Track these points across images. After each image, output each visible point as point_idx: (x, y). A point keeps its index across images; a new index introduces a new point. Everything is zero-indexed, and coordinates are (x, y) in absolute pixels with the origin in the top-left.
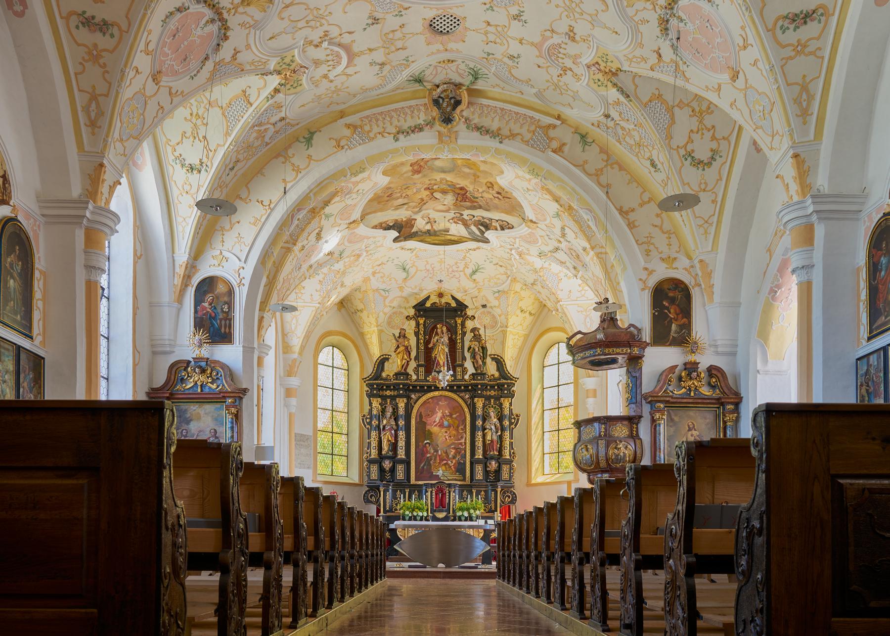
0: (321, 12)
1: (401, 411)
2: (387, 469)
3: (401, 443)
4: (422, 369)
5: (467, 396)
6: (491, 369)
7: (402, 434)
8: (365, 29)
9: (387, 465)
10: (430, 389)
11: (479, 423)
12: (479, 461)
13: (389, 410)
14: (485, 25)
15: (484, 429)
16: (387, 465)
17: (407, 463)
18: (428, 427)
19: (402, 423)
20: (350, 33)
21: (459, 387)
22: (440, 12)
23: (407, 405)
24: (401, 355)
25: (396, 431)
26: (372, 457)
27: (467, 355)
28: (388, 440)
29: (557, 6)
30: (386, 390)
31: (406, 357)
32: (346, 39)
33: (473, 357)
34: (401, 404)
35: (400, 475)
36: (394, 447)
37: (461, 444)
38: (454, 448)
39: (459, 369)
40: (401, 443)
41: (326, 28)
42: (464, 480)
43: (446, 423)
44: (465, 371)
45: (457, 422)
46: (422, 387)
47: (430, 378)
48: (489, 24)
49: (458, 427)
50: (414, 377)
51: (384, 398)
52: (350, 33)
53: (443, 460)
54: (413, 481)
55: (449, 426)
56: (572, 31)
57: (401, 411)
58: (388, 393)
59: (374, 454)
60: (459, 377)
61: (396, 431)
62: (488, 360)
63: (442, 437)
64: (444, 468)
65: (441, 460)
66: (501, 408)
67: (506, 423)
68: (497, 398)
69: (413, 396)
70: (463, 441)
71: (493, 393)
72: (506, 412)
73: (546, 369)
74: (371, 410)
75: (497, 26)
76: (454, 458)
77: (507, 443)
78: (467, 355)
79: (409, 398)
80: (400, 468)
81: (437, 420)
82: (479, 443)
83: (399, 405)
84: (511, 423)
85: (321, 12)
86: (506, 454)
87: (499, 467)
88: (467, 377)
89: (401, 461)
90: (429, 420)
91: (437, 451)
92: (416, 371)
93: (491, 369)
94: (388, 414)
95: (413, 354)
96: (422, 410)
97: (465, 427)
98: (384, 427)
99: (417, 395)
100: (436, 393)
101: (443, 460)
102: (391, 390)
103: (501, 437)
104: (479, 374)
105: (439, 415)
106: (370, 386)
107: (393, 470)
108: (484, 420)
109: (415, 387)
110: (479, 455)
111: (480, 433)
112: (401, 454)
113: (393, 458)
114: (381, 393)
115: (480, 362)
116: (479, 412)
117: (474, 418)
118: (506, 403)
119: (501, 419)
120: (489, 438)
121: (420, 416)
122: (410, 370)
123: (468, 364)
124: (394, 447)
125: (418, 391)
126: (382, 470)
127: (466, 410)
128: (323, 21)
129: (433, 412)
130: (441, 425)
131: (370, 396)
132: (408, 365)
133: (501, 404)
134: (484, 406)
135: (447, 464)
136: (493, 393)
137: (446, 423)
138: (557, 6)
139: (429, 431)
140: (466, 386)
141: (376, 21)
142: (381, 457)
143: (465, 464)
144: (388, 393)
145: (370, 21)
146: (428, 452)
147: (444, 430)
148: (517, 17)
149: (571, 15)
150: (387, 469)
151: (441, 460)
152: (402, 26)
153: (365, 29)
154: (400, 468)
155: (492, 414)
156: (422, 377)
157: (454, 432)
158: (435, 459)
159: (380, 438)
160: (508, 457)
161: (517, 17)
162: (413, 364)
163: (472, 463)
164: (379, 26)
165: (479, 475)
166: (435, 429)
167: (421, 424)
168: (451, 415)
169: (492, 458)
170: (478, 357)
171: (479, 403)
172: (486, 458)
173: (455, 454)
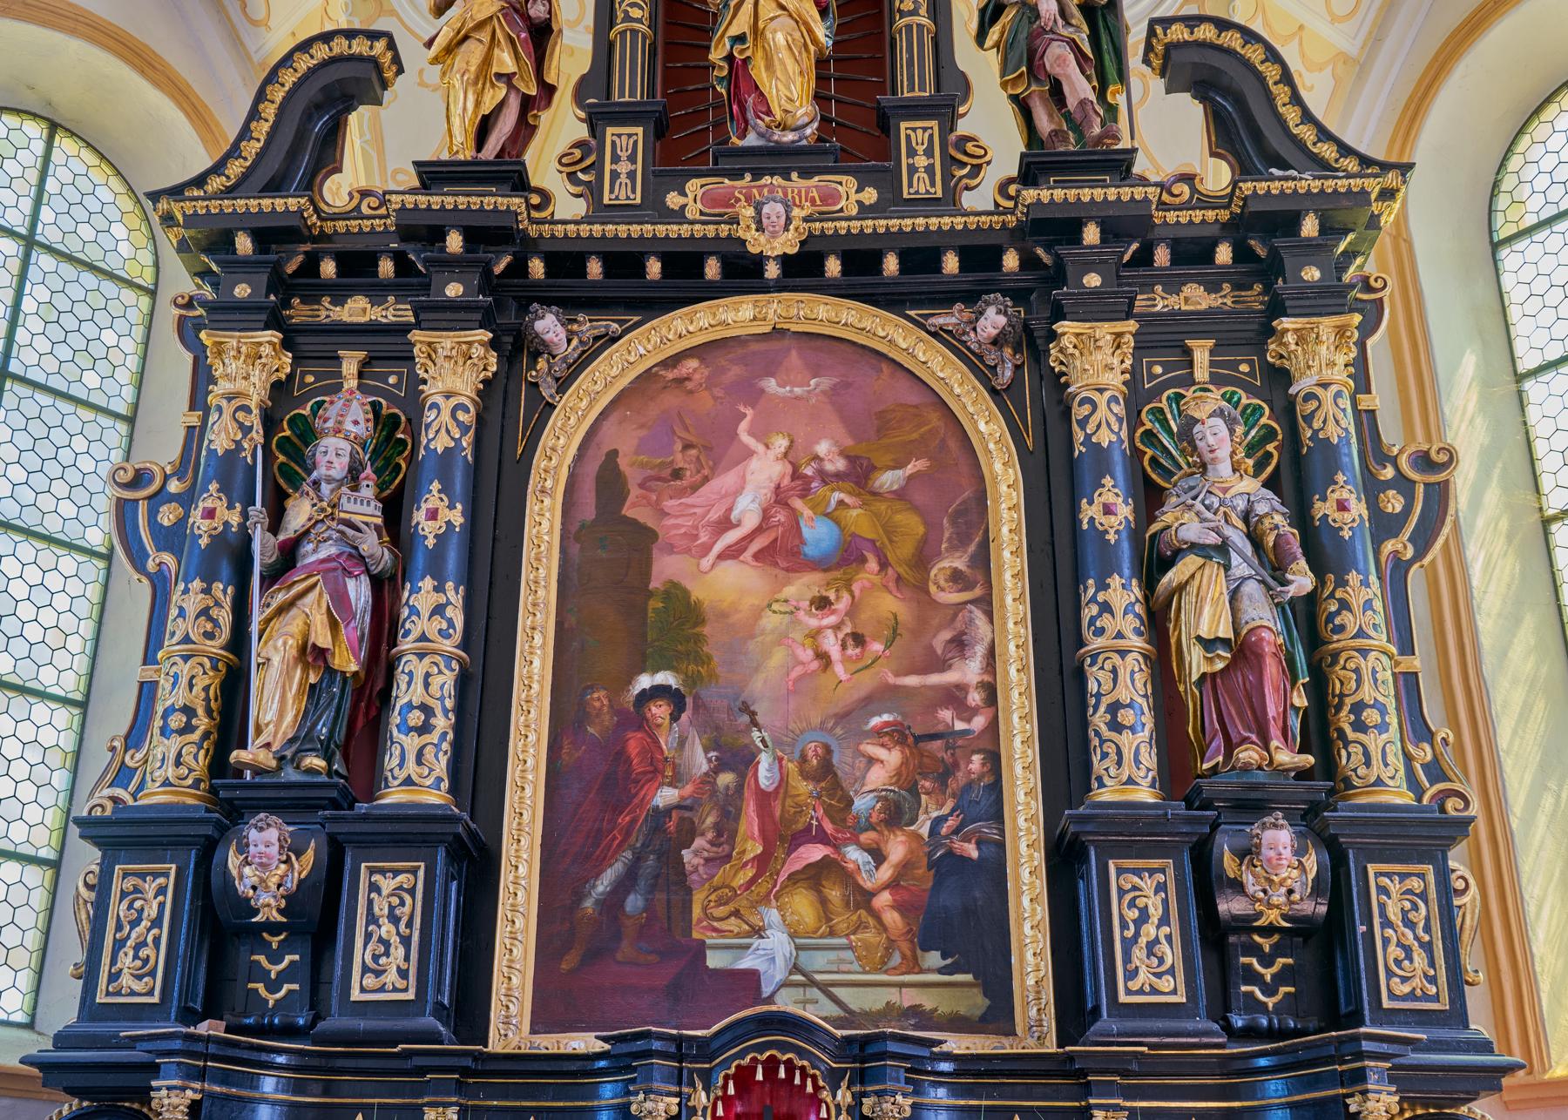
1: (445, 431)
2: (269, 907)
3: (426, 682)
4: (627, 139)
5: (993, 320)
6: (1168, 136)
7: (433, 612)
9: (265, 865)
10: (687, 276)
11: (1109, 509)
12: (1132, 833)
13: (345, 424)
15: (1154, 560)
16: (265, 865)
17: (472, 863)
18: (666, 568)
19: (438, 515)
21: (921, 257)
23: (497, 399)
24: (473, 53)
25: (386, 589)
26: (156, 796)
27: (981, 65)
28: (311, 655)
30: (340, 293)
31: (505, 61)
33: (1025, 60)
34: (453, 370)
35: (383, 959)
36: (359, 707)
37: (954, 696)
38: (897, 735)
39: (915, 134)
40: (426, 682)
42: (999, 1016)
43: (818, 534)
44: (960, 159)
45: (911, 524)
46: (624, 262)
47: (691, 196)
49: (923, 559)
50: (568, 206)
51: (311, 347)
53: (802, 837)
54: (511, 1024)
55: (849, 555)
57: (445, 431)
58: (357, 310)
59: (170, 772)
60: (920, 186)
61: (386, 589)
62: (1145, 83)
63: (785, 642)
64: (802, 904)
65: (783, 835)
66: (1288, 412)
67: (1344, 507)
68: (1248, 336)
69: (548, 325)
70: (969, 671)
71: (1195, 298)
72: (1334, 421)
73: (1510, 259)
74: (194, 436)
76: (896, 814)
77: (1370, 676)
78: (981, 65)
79: (516, 347)
80: (389, 912)
81: (748, 510)
82: (1121, 678)
83: (432, 391)
84: (1384, 526)
86: (1383, 770)
87: (1337, 885)
88: (980, 198)
89: (407, 834)
90: (678, 516)
91: (739, 759)
92: (584, 163)
93: (1168, 136)
94: (332, 456)
95: (573, 55)
96: (624, 440)
97: (983, 559)
98: (289, 555)
99: (588, 326)
100: (739, 314)
101: (802, 837)
102: (377, 291)
103: (1309, 622)
104: (1070, 151)
105: (764, 469)
106: (211, 244)
107: (319, 918)
108: (1149, 497)
109: (566, 261)
110: (1128, 773)
111: (1123, 593)
112: (416, 772)
113: (339, 808)
114: (299, 312)
115: (1079, 87)
116: (1103, 425)
117: (1056, 476)
118: (1317, 353)
119: (1295, 470)
120: (1206, 615)
121: (602, 482)
122: (543, 164)
123: (992, 123)
124: (359, 707)
125: (595, 303)
126: (216, 926)
127: (987, 425)
129: (718, 450)
130: (779, 550)
131: (202, 321)
132: (525, 129)
133: (1279, 377)
134: (1136, 396)
135: (827, 869)
136: (1195, 298)
137: (818, 534)
139: (676, 594)
140: (980, 255)
142: (232, 798)
143: (994, 870)
144: (357, 310)
146: (658, 768)
147: (802, 587)
150: (269, 907)
151: (783, 835)
154: (389, 912)
155: (1217, 438)
156: (624, 191)
157: (889, 604)
158: (726, 832)
159: (239, 642)
160: (1398, 795)
162: (562, 125)
163: (1066, 859)
165: (1151, 961)
166: (725, 583)
167: (613, 547)
168: (859, 474)
169: (1251, 805)
170: (1060, 60)
171: (1096, 358)
172: (1199, 822)
173: (908, 782)
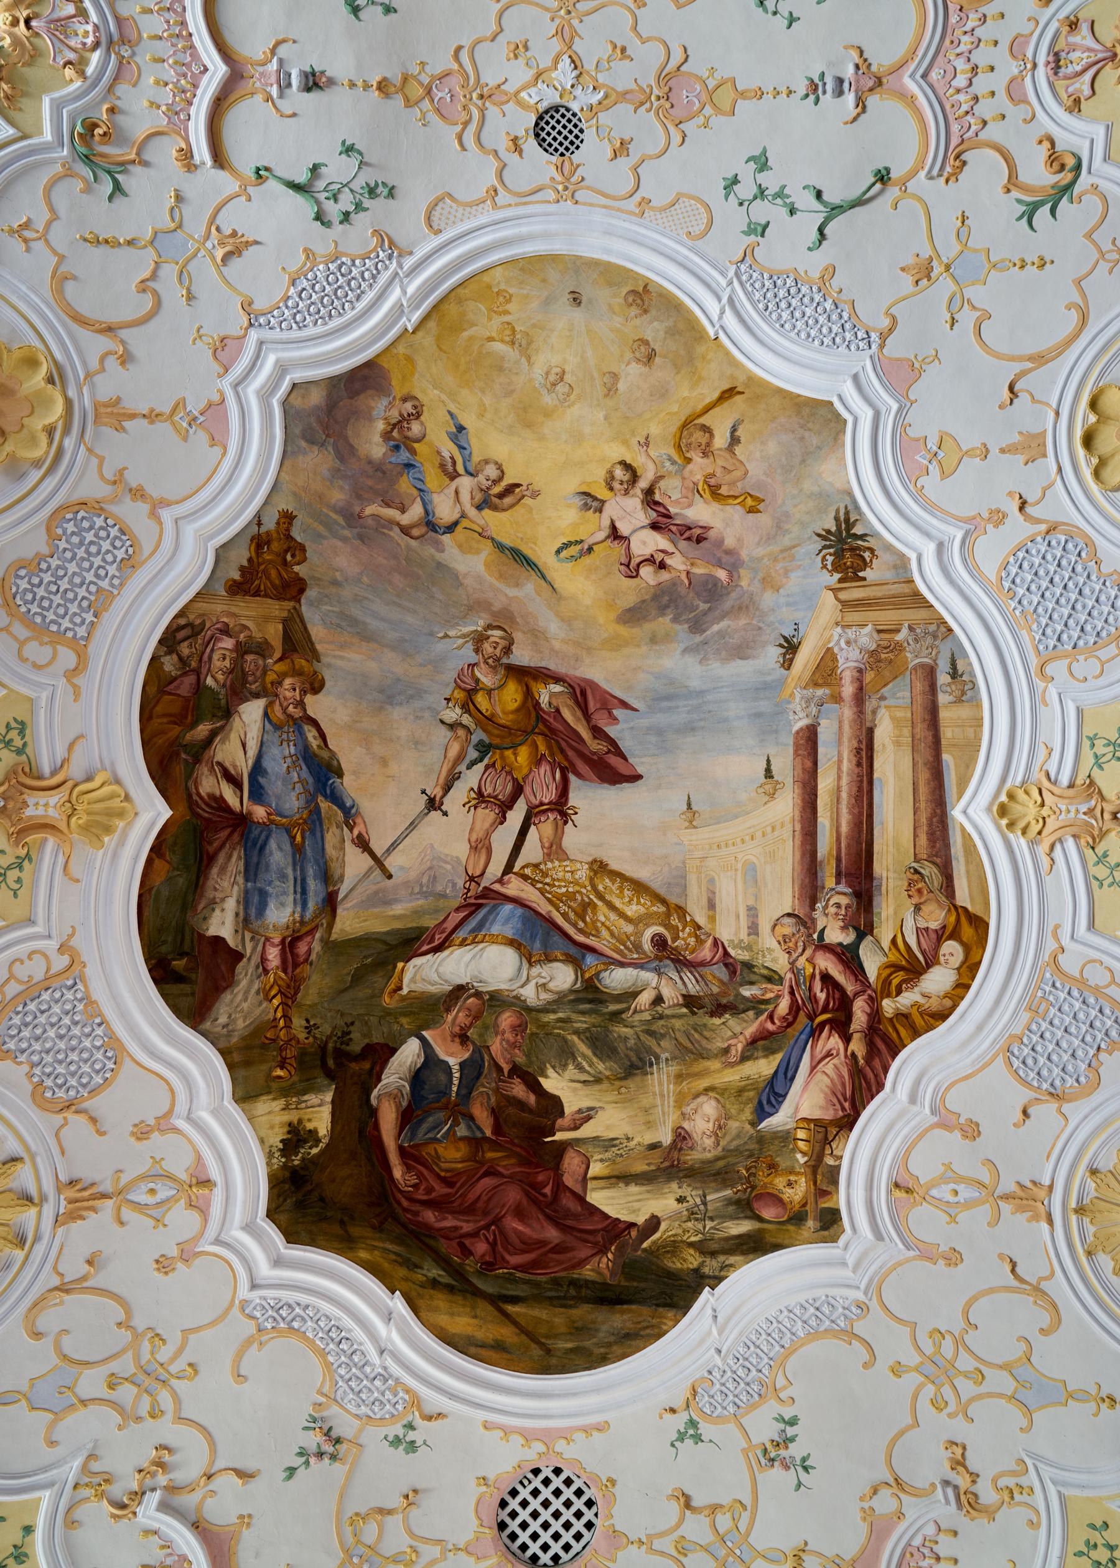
0: (164, 1354)
8: (291, 1471)
14: (675, 1508)
20: (241, 1474)
22: (532, 1455)
29: (897, 1370)
32: (224, 1503)
41: (167, 1430)
48: (687, 1503)
52: (241, 1474)
56: (959, 1463)
75: (715, 1508)
85: (164, 1354)
128: (165, 1398)
138: (897, 1370)
141: (332, 1444)
145: (313, 1440)
148: (774, 1453)
149: (947, 1391)
152: (412, 1497)
153: (291, 1471)
161: (774, 1453)
164: (339, 1469)
